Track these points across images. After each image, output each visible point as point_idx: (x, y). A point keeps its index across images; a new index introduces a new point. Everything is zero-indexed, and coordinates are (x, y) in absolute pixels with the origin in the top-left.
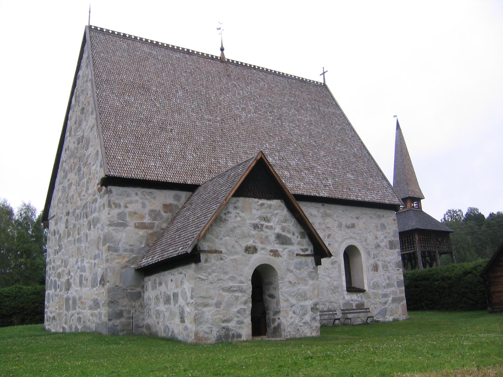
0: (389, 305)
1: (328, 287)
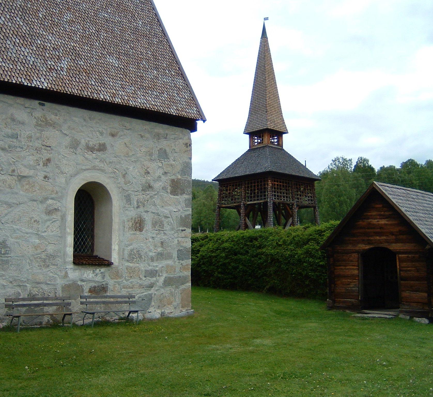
0: (157, 290)
1: (33, 255)
